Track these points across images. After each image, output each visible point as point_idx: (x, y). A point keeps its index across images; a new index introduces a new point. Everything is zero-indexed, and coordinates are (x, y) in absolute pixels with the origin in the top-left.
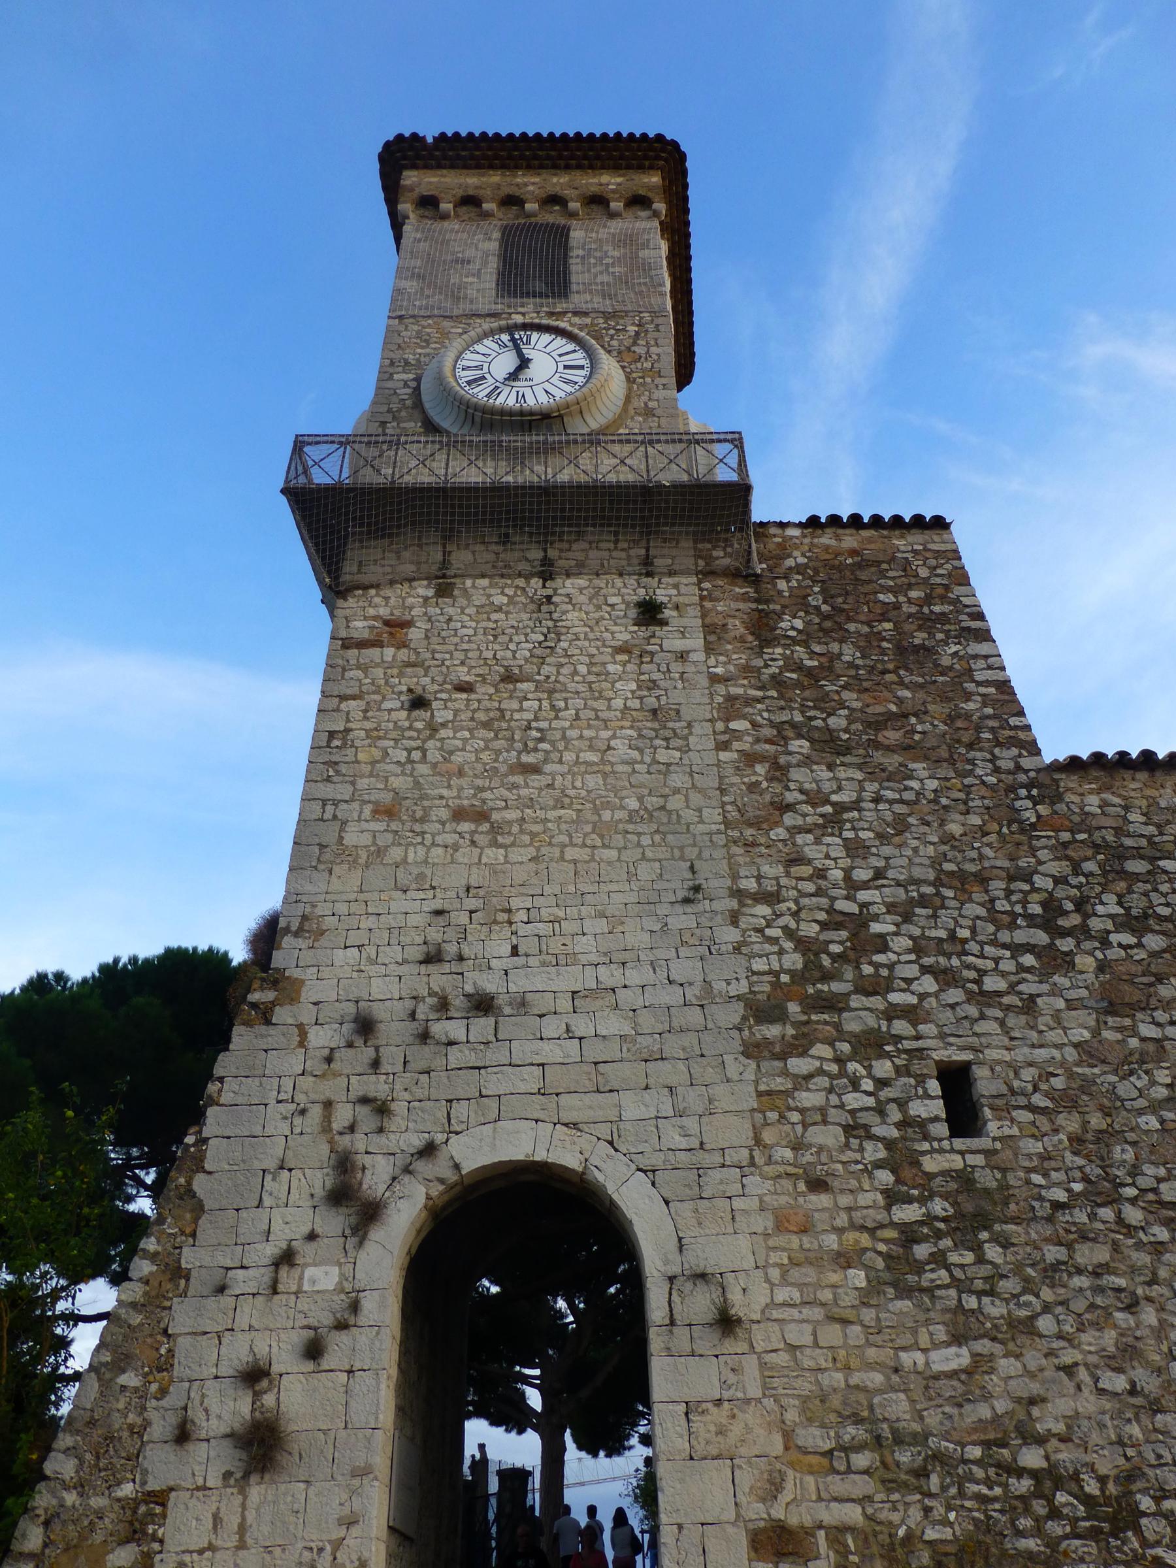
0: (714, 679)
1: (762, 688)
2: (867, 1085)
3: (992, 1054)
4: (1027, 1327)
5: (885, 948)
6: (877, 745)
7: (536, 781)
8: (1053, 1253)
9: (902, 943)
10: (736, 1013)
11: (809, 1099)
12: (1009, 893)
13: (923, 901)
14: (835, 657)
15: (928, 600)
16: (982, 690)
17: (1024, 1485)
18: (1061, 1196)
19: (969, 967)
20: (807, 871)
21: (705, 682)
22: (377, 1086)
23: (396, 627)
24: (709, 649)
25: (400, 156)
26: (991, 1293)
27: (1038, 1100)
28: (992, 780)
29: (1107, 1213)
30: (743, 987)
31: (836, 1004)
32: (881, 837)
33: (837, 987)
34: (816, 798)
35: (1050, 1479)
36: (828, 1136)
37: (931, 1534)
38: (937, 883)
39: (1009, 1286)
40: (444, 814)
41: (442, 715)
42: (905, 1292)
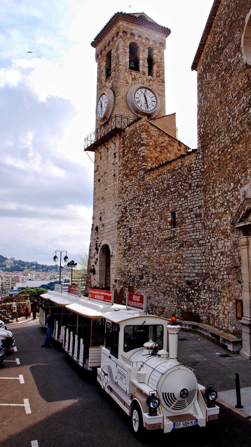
0: (119, 166)
1: (122, 167)
2: (124, 232)
3: (133, 226)
4: (131, 260)
5: (127, 212)
6: (131, 175)
7: (107, 191)
8: (134, 252)
9: (128, 210)
10: (117, 223)
11: (121, 234)
12: (137, 199)
13: (130, 203)
14: (129, 156)
15: (138, 139)
16: (141, 158)
17: (129, 277)
18: (135, 245)
19: (133, 213)
20: (123, 200)
21: (118, 167)
22: (98, 236)
23: (98, 167)
24: (119, 161)
25: (94, 44)
26: (129, 257)
27: (136, 232)
28: (139, 178)
29: (138, 247)
30: (117, 220)
31: (123, 221)
32: (129, 192)
33: (124, 218)
34: (125, 187)
35: (131, 276)
36: (121, 239)
37: (123, 281)
38: (132, 200)
39: (131, 256)
40: (101, 198)
41: (101, 182)
42: (124, 257)
